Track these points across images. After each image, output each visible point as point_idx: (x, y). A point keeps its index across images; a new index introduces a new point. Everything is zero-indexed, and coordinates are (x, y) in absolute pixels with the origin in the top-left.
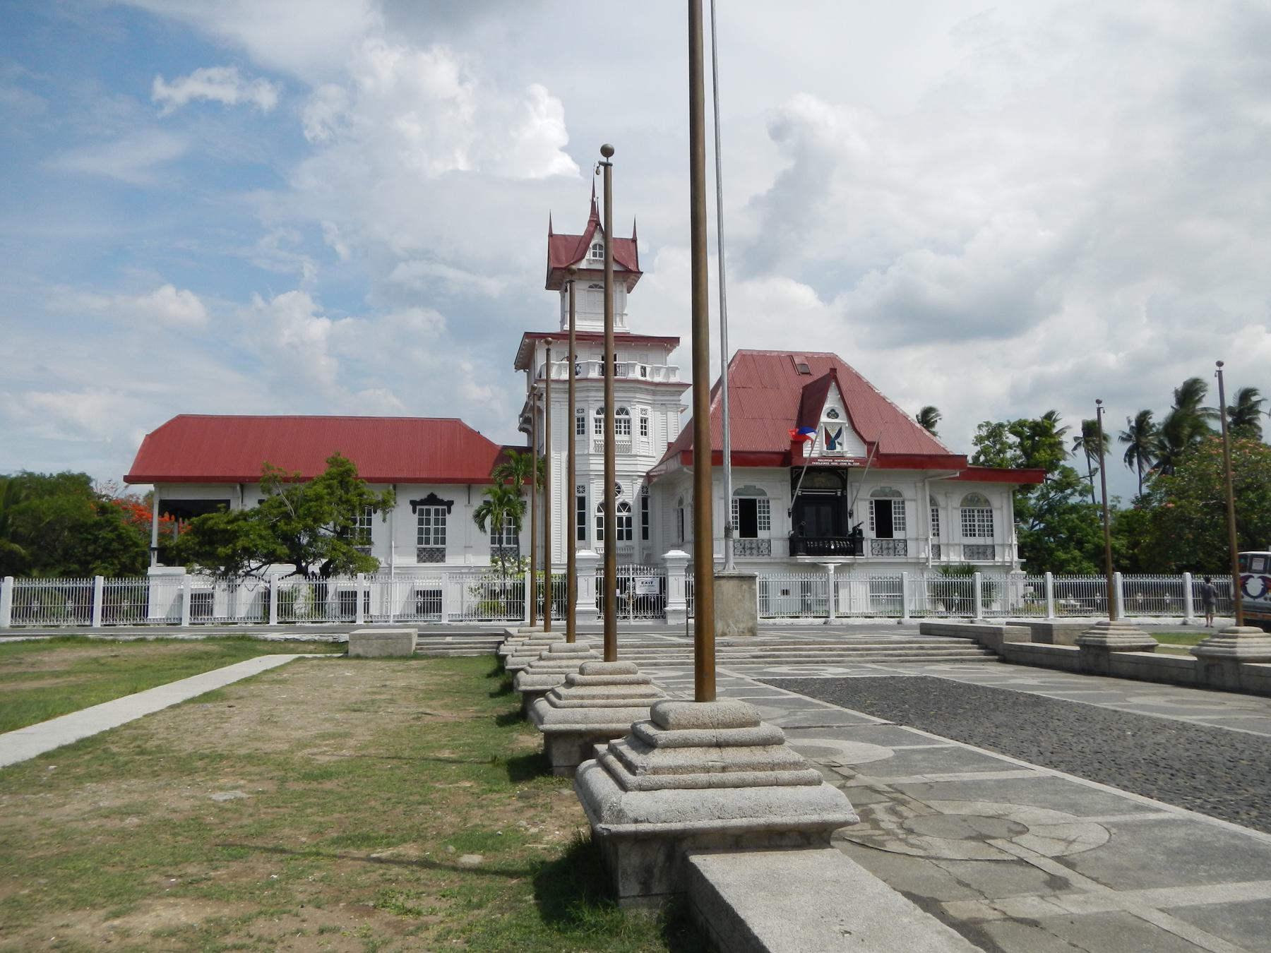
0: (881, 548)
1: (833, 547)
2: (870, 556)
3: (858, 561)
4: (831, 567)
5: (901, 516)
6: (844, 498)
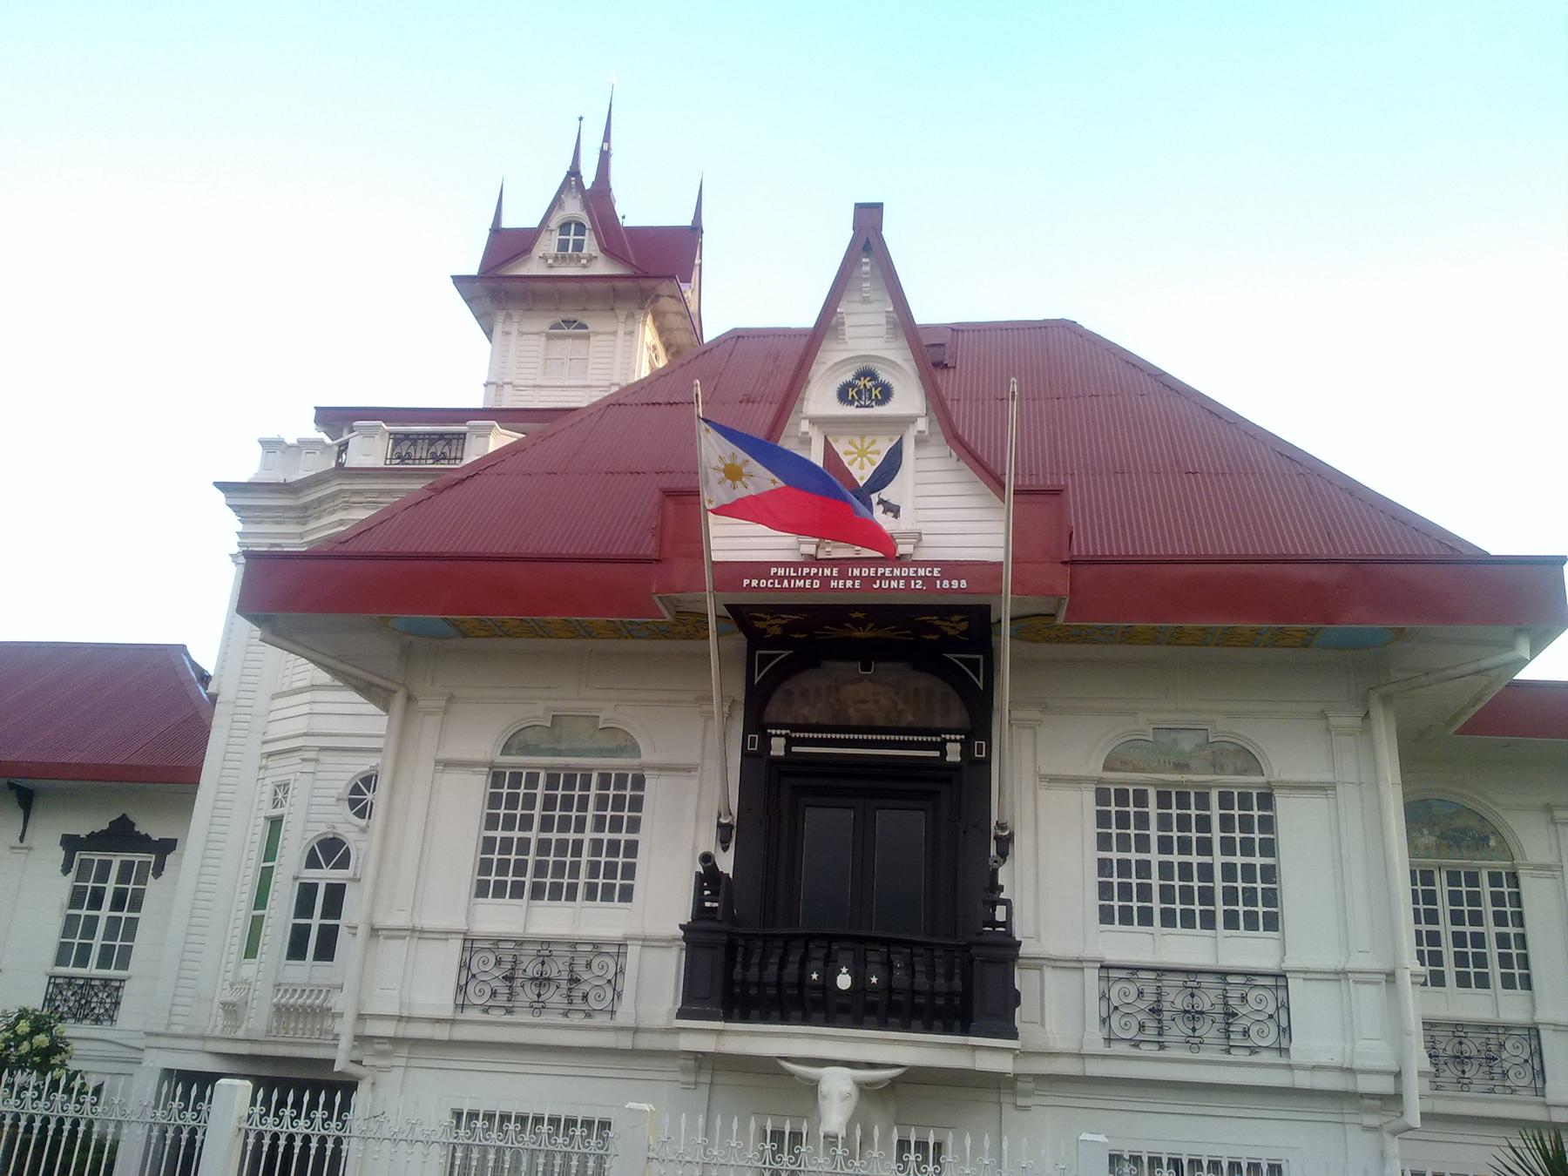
0: (1156, 1011)
1: (844, 981)
2: (1095, 1043)
3: (988, 1063)
4: (837, 1086)
5: (1258, 860)
6: (976, 771)
